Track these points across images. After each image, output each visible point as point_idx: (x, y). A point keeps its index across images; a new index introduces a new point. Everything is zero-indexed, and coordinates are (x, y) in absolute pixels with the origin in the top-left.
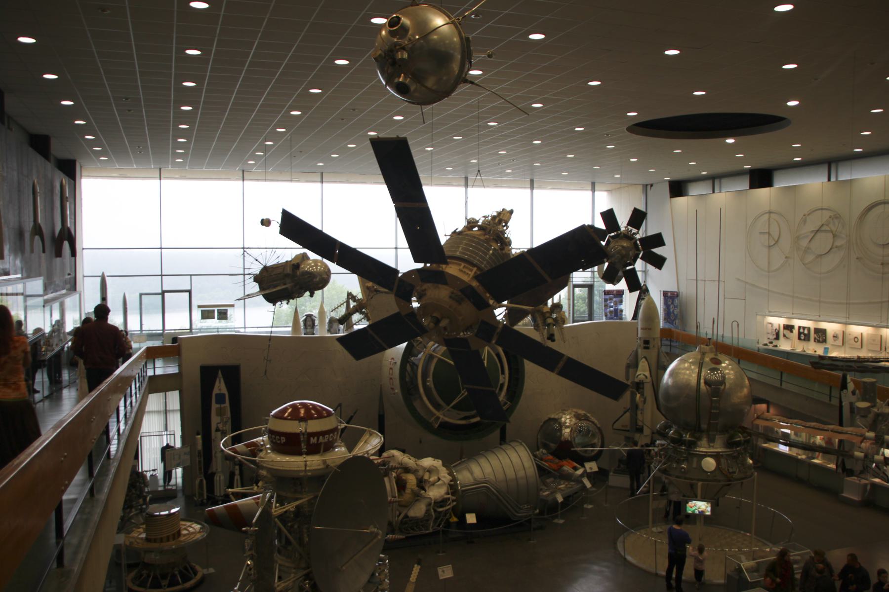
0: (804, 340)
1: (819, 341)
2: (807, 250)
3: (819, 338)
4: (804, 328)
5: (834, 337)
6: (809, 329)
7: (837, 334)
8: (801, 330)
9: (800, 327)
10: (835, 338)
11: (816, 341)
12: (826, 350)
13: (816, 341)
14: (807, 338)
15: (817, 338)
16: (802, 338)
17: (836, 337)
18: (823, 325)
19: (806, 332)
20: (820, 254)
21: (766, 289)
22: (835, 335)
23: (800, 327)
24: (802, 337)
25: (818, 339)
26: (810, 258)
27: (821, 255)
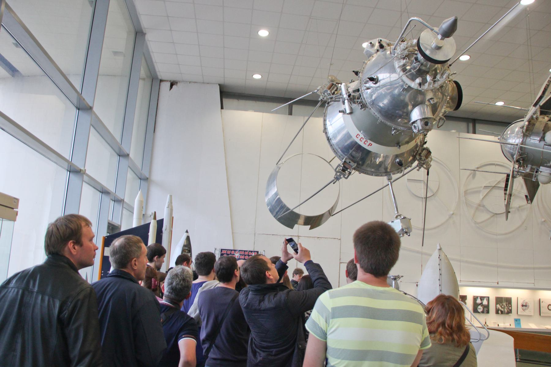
0: (483, 312)
1: (502, 313)
2: (481, 207)
3: (504, 308)
4: (482, 298)
5: (523, 306)
6: (488, 298)
7: (526, 303)
8: (479, 301)
9: (475, 298)
10: (524, 307)
11: (500, 312)
12: (517, 321)
13: (500, 312)
14: (486, 310)
15: (500, 308)
16: (480, 311)
17: (526, 306)
18: (506, 293)
19: (485, 302)
20: (496, 213)
21: (418, 252)
22: (524, 304)
23: (475, 298)
24: (480, 309)
25: (502, 310)
26: (483, 217)
27: (496, 214)
